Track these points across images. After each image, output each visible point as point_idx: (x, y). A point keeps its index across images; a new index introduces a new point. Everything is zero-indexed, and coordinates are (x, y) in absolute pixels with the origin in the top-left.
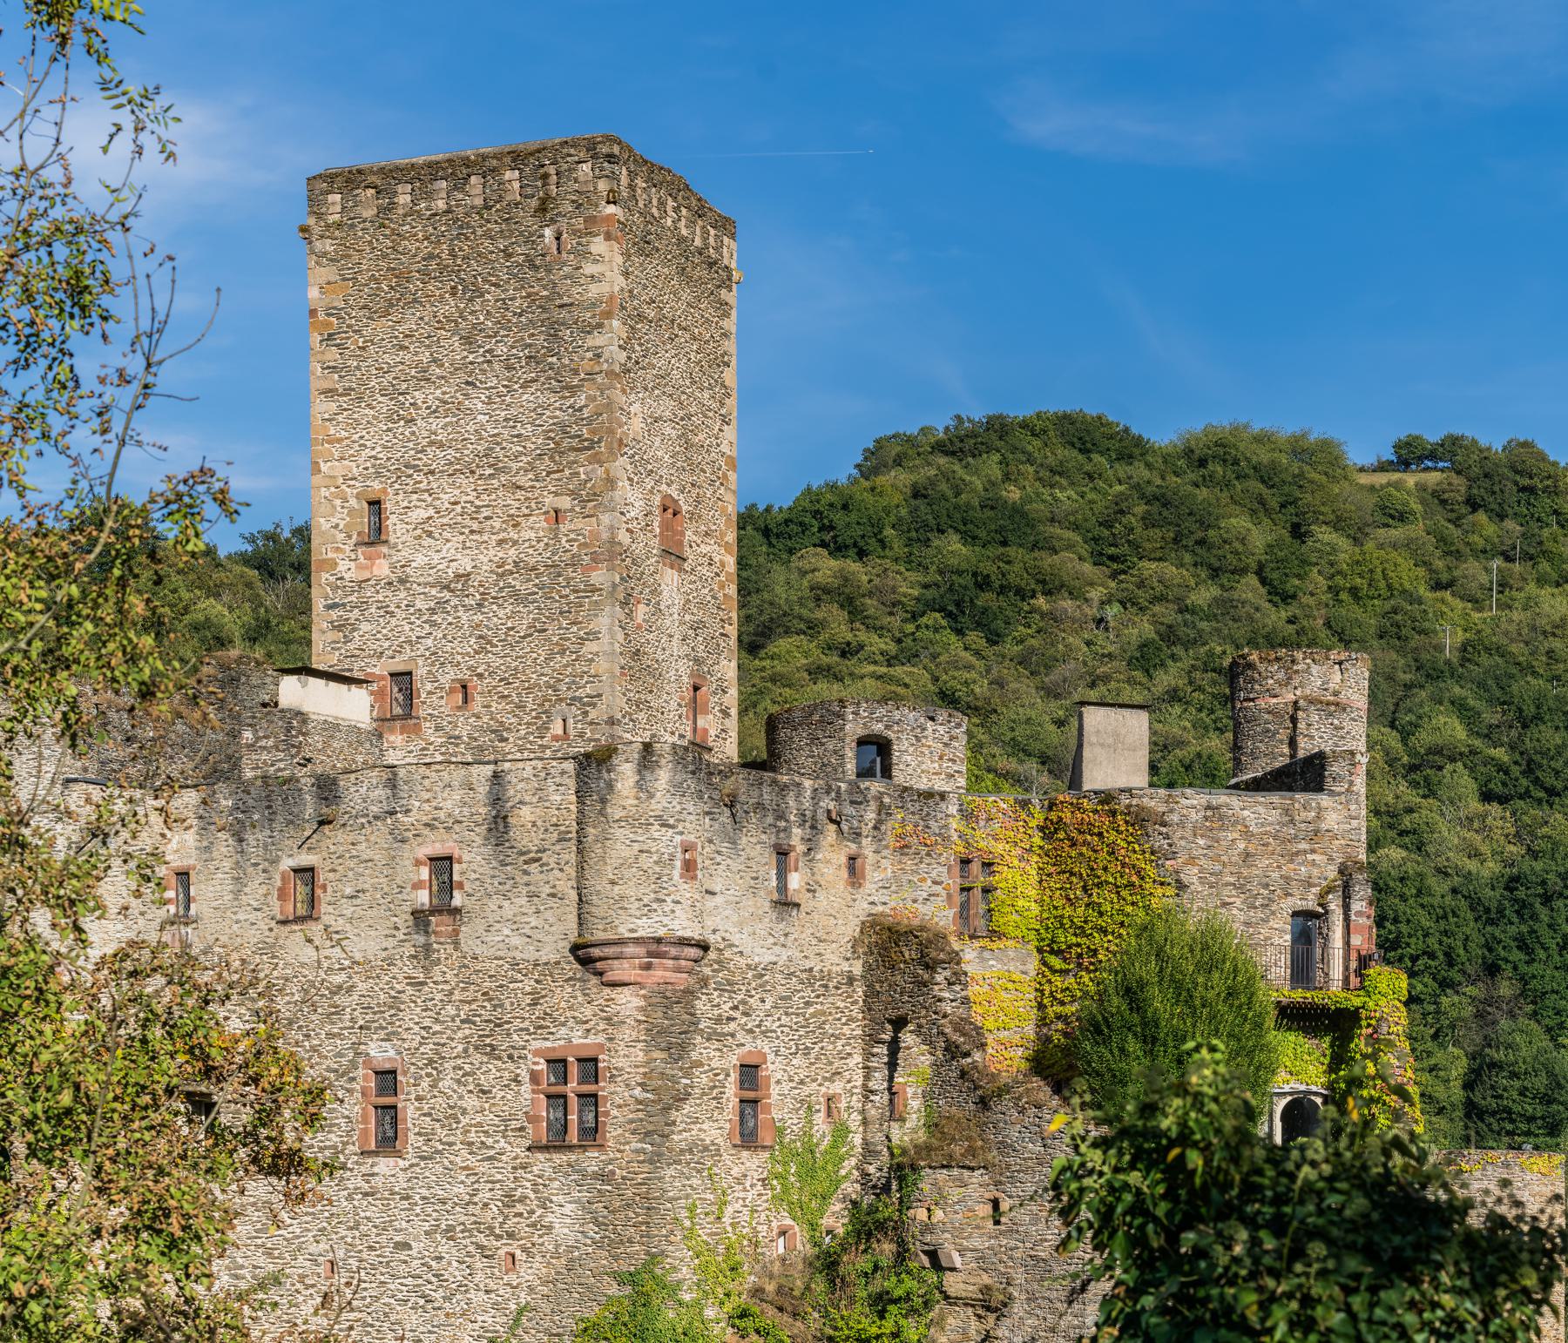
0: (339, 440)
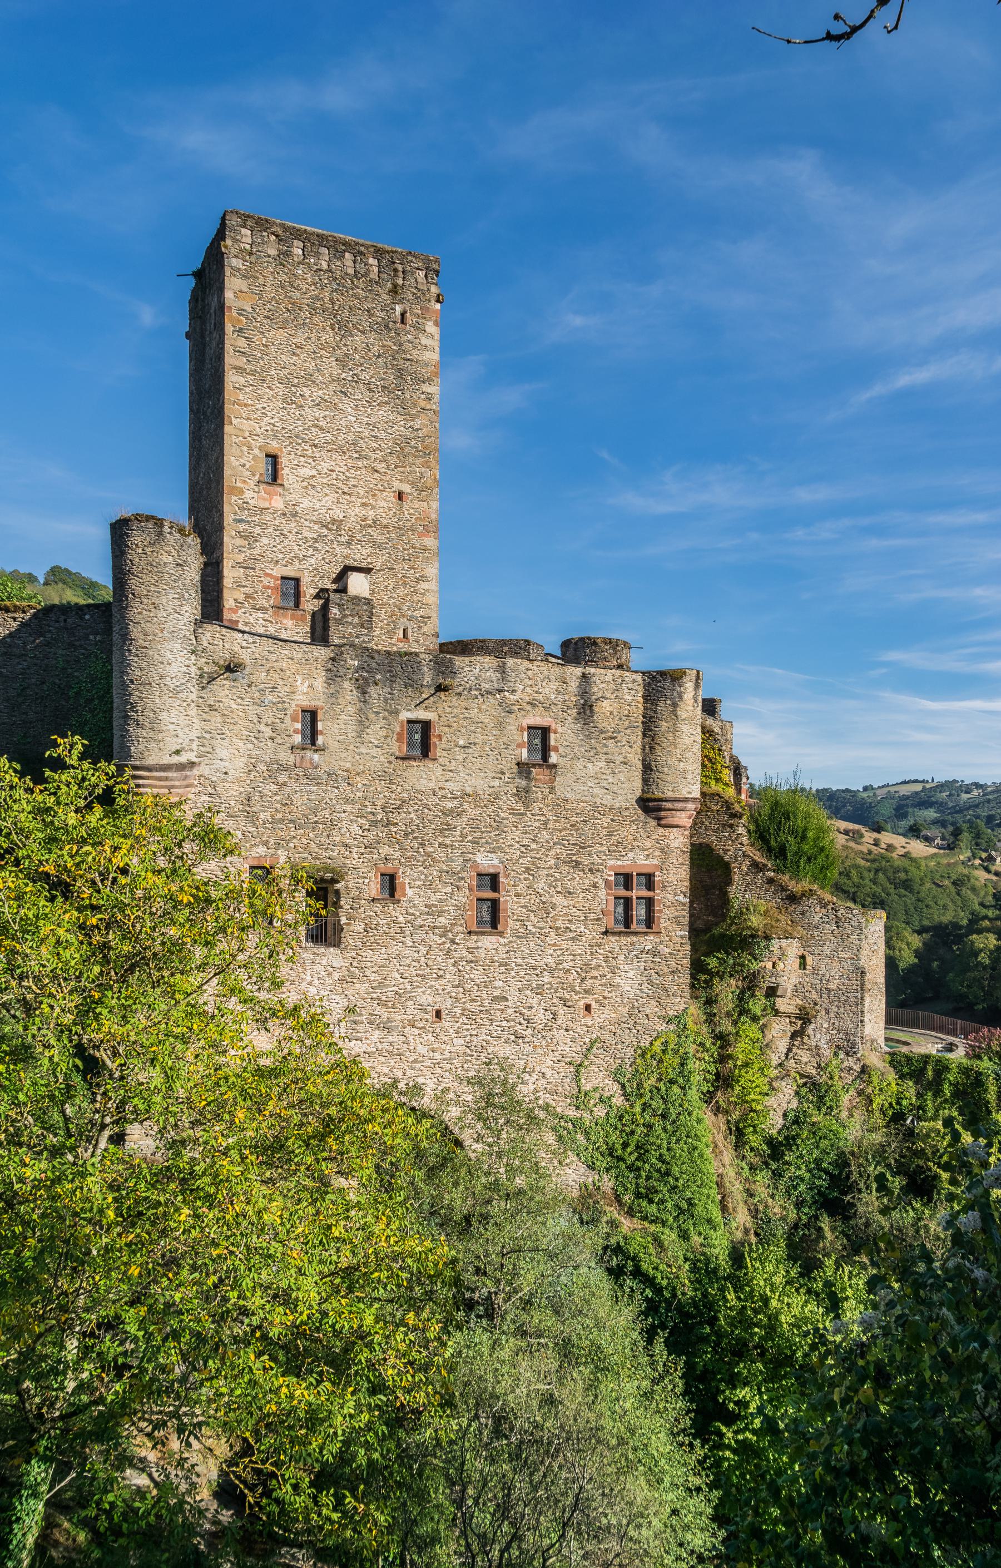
0: (246, 405)
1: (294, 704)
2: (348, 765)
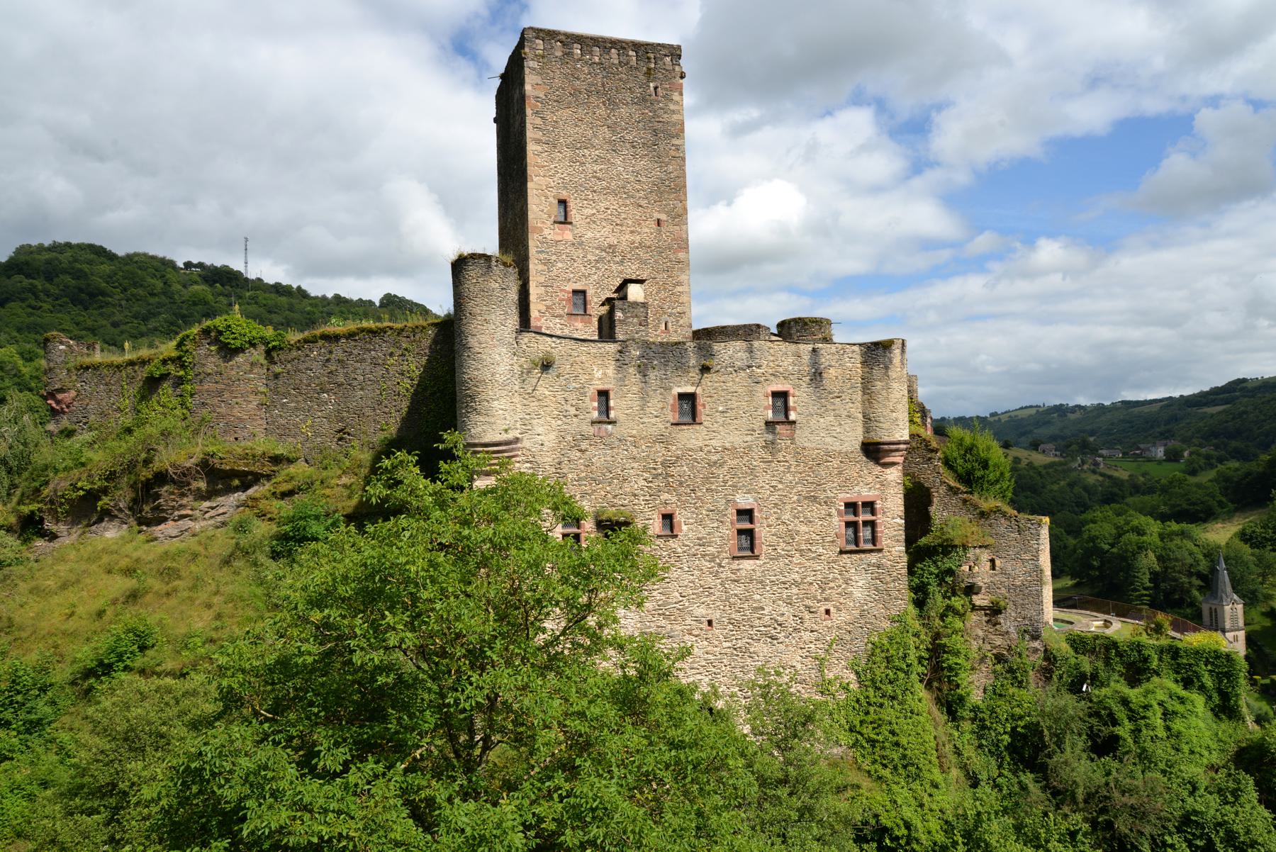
1: (591, 387)
2: (634, 432)
